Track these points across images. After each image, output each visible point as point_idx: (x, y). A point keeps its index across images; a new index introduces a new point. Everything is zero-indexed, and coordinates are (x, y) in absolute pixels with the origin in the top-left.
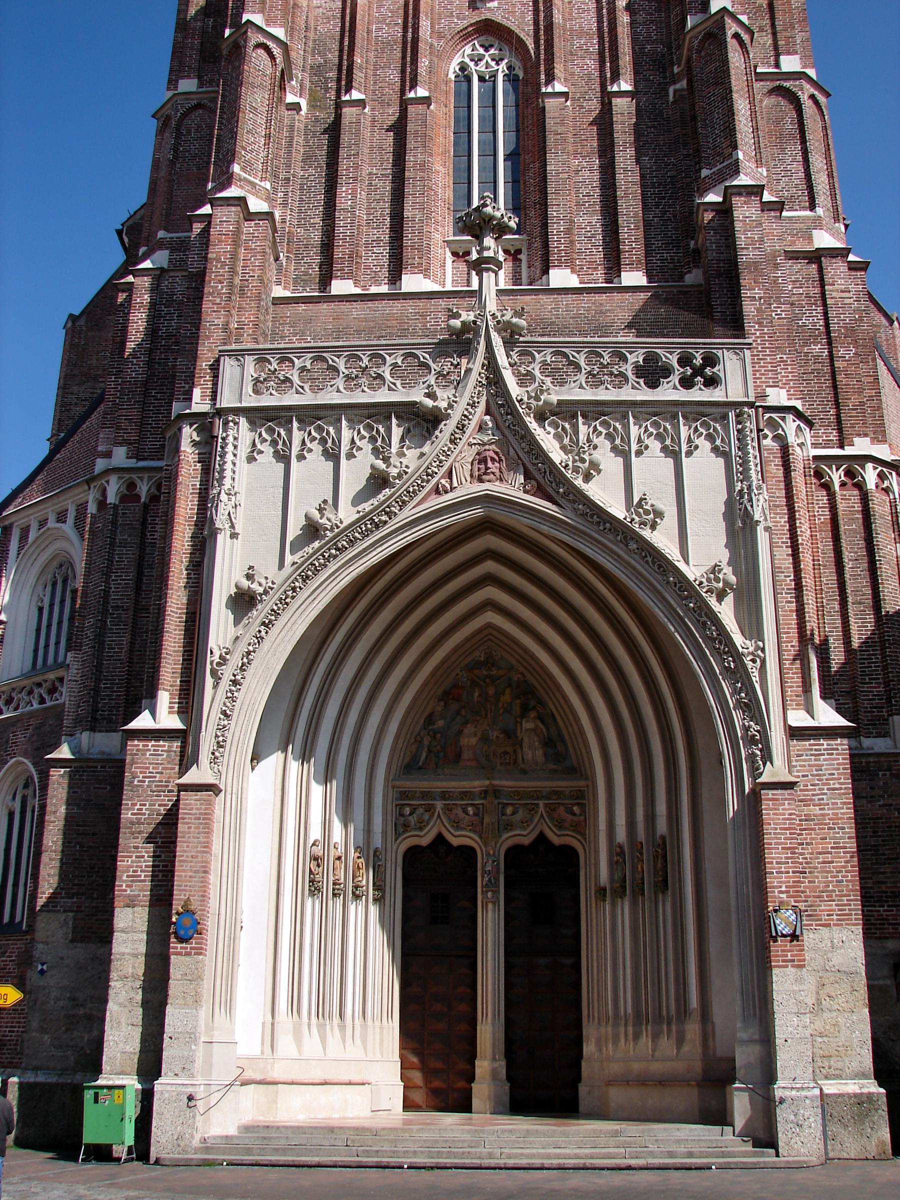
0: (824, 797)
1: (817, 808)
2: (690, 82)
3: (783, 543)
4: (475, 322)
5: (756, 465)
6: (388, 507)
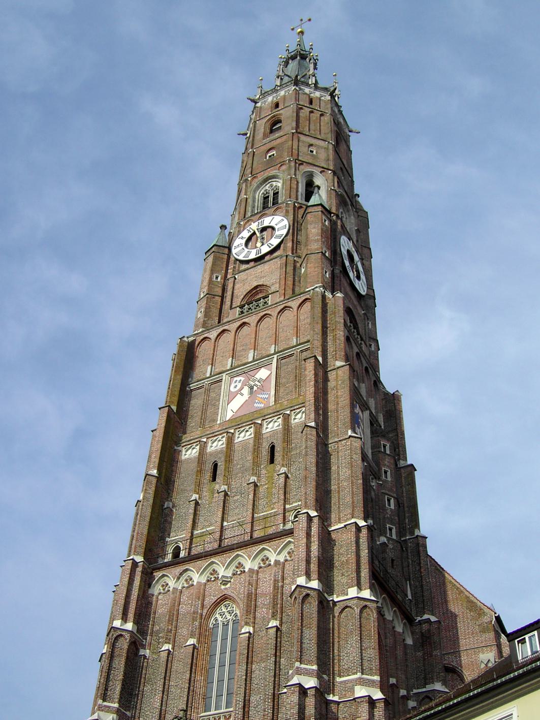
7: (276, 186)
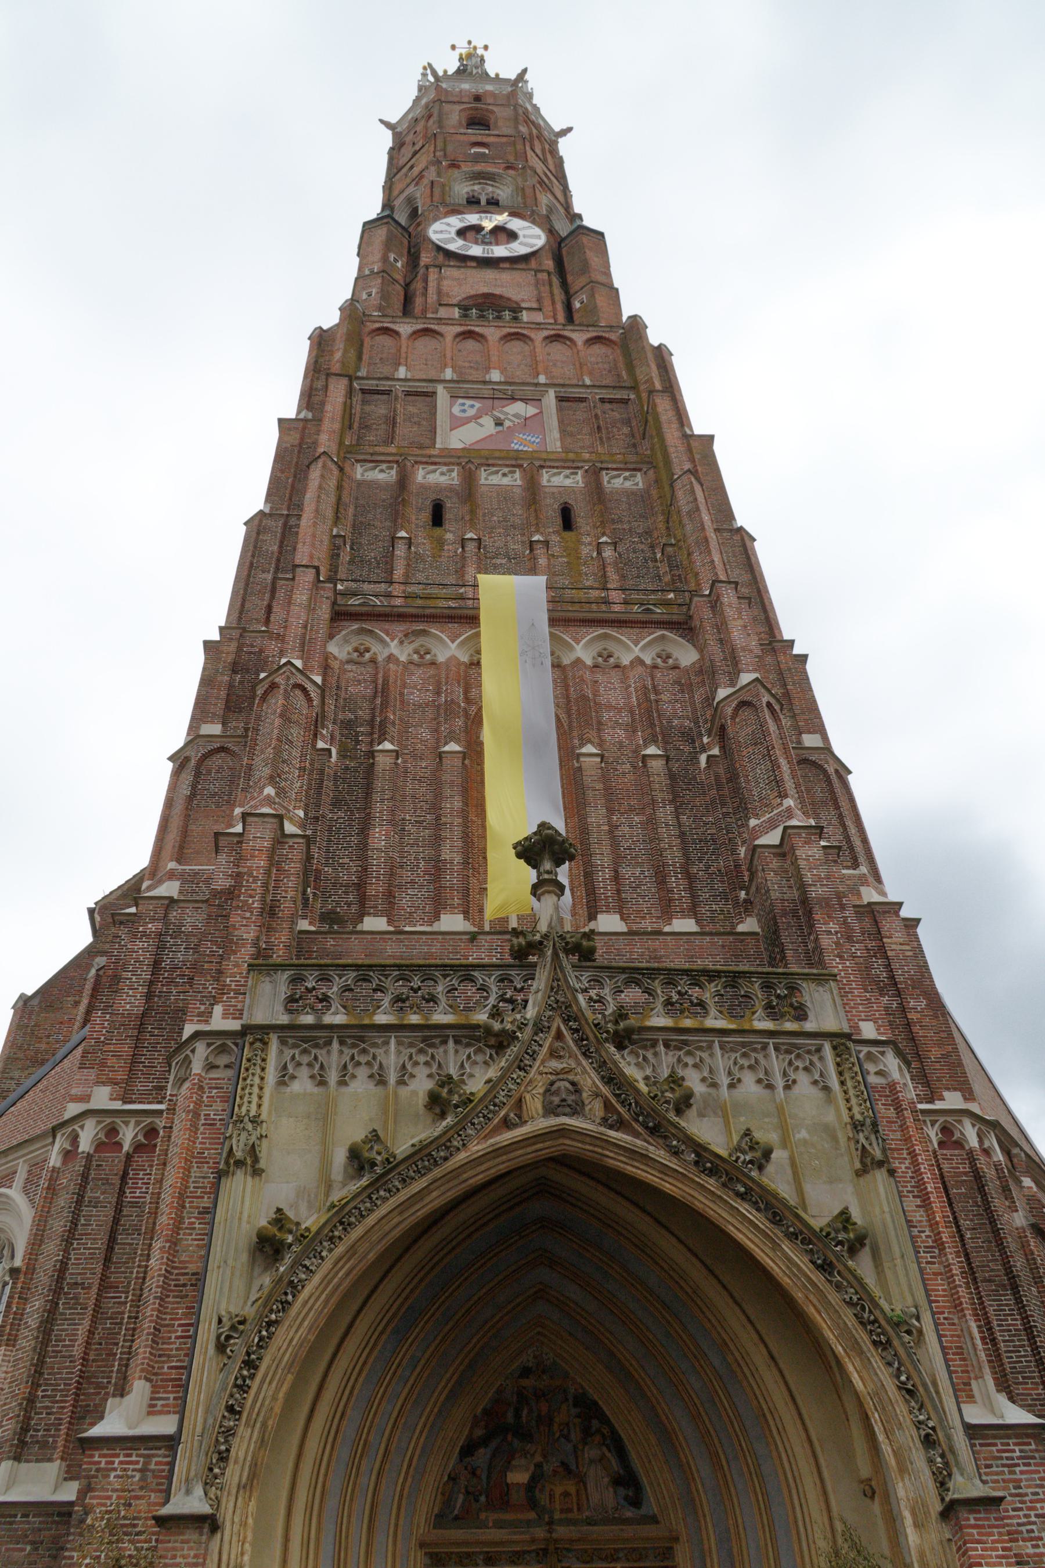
0: (1034, 1527)
1: (1029, 1544)
2: (723, 748)
4: (541, 943)
6: (449, 1140)
7: (493, 192)
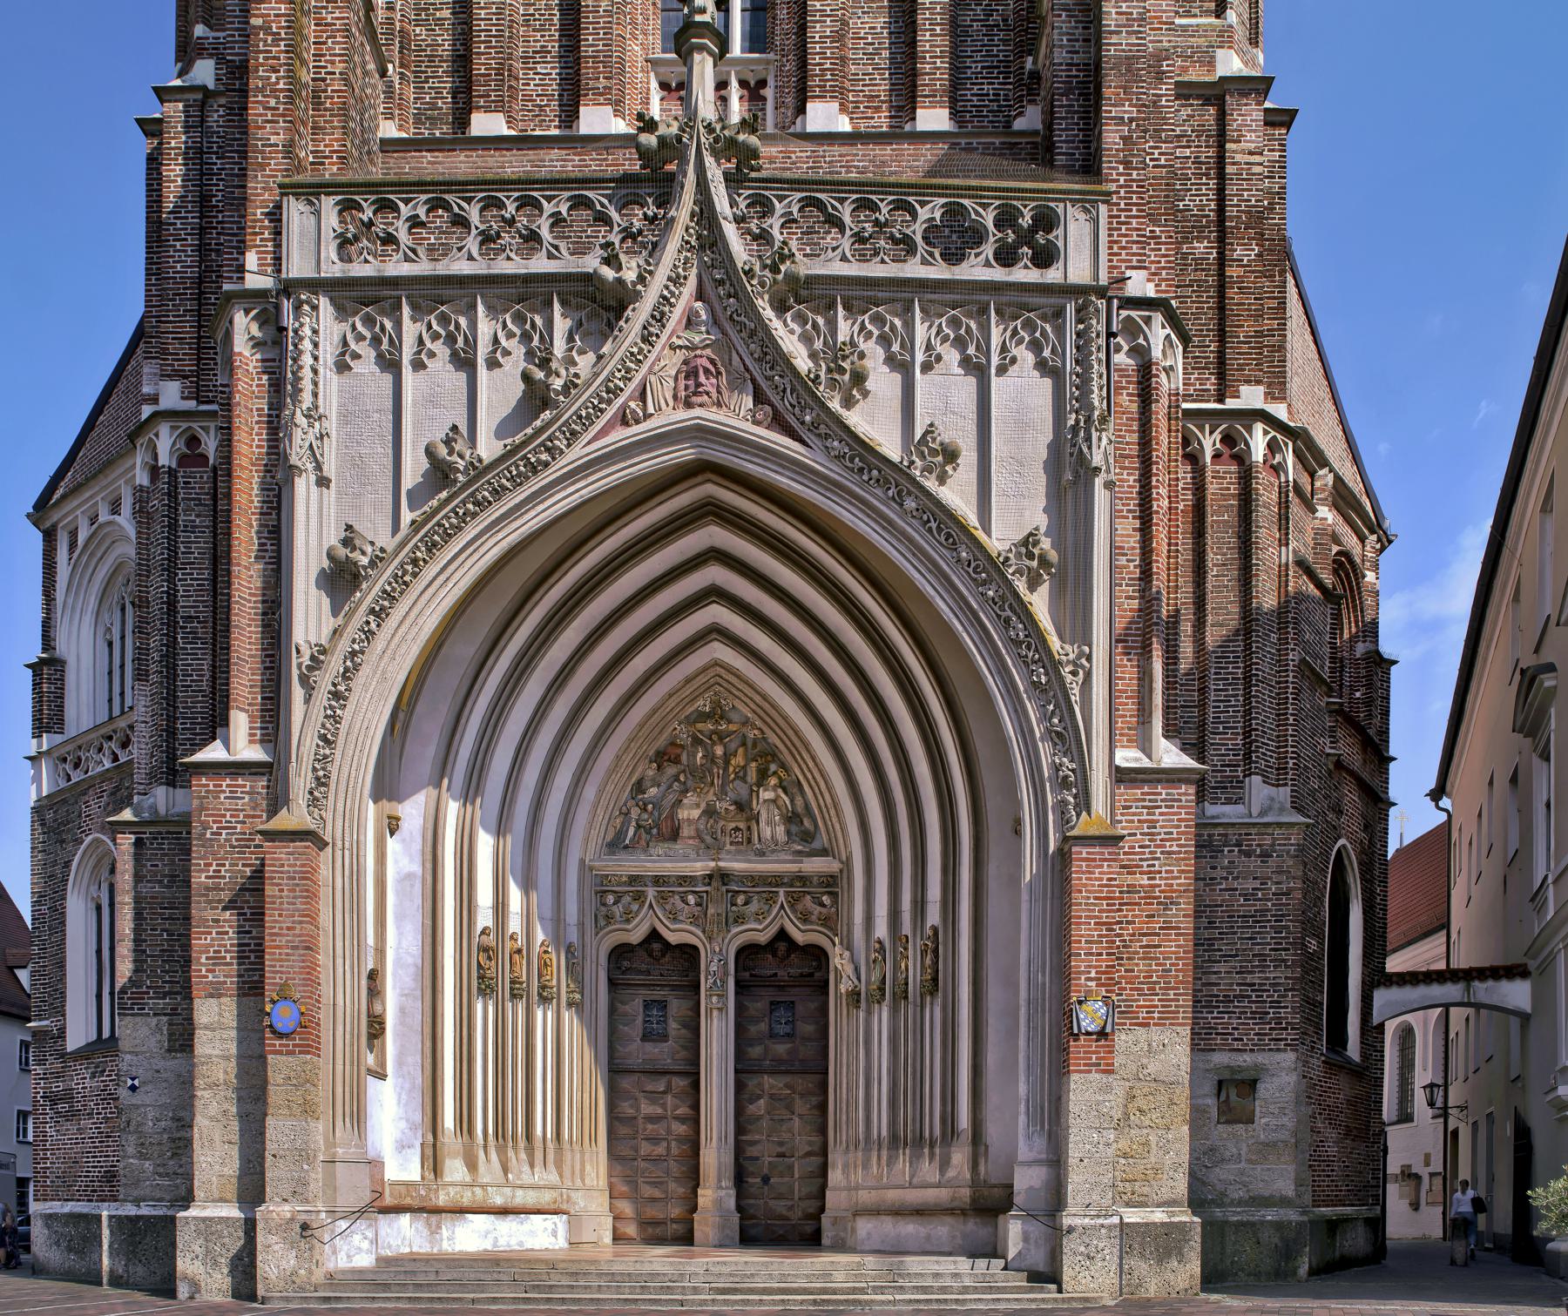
3: (1129, 511)
5: (1101, 389)
